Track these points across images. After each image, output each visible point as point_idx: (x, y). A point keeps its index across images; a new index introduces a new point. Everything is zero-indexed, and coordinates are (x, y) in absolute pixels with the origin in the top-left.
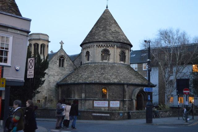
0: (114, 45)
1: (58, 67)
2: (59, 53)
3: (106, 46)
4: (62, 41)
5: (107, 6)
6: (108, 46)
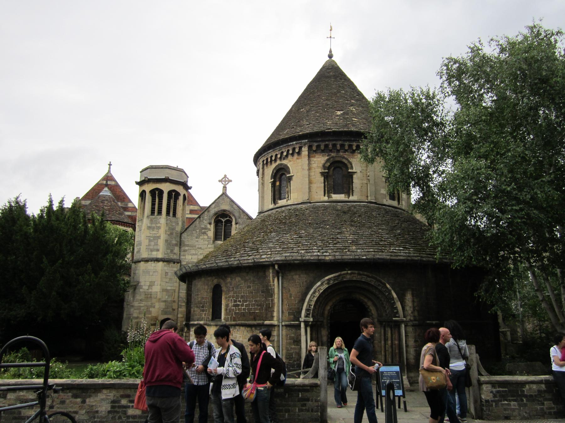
0: (300, 148)
1: (212, 242)
2: (214, 205)
3: (279, 156)
4: (225, 176)
5: (331, 51)
6: (285, 154)
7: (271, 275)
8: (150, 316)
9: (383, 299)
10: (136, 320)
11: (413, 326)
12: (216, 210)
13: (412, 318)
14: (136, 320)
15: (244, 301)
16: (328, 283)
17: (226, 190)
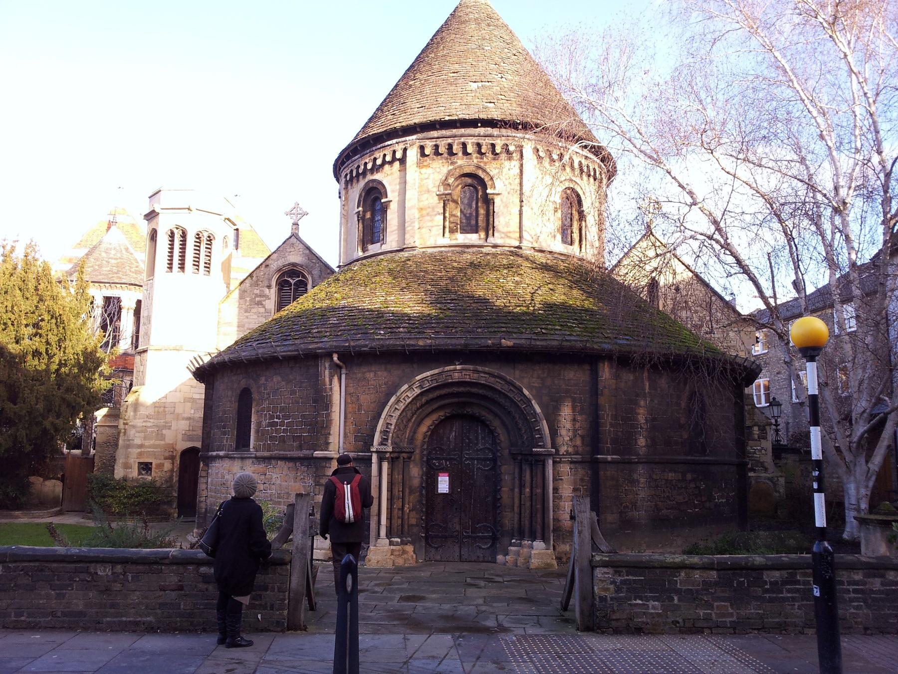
2: (275, 255)
7: (327, 372)
8: (163, 442)
9: (517, 416)
10: (139, 450)
11: (572, 462)
12: (281, 263)
13: (570, 450)
14: (139, 450)
15: (286, 417)
16: (421, 387)
17: (297, 229)
